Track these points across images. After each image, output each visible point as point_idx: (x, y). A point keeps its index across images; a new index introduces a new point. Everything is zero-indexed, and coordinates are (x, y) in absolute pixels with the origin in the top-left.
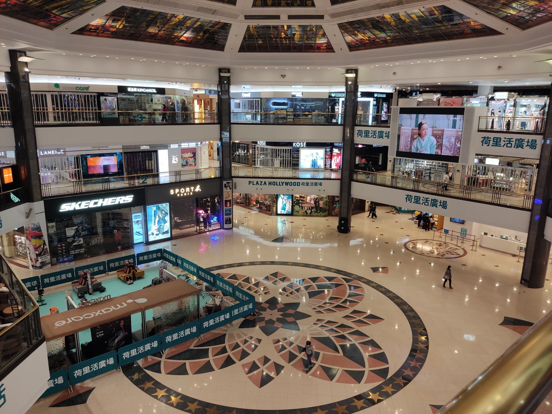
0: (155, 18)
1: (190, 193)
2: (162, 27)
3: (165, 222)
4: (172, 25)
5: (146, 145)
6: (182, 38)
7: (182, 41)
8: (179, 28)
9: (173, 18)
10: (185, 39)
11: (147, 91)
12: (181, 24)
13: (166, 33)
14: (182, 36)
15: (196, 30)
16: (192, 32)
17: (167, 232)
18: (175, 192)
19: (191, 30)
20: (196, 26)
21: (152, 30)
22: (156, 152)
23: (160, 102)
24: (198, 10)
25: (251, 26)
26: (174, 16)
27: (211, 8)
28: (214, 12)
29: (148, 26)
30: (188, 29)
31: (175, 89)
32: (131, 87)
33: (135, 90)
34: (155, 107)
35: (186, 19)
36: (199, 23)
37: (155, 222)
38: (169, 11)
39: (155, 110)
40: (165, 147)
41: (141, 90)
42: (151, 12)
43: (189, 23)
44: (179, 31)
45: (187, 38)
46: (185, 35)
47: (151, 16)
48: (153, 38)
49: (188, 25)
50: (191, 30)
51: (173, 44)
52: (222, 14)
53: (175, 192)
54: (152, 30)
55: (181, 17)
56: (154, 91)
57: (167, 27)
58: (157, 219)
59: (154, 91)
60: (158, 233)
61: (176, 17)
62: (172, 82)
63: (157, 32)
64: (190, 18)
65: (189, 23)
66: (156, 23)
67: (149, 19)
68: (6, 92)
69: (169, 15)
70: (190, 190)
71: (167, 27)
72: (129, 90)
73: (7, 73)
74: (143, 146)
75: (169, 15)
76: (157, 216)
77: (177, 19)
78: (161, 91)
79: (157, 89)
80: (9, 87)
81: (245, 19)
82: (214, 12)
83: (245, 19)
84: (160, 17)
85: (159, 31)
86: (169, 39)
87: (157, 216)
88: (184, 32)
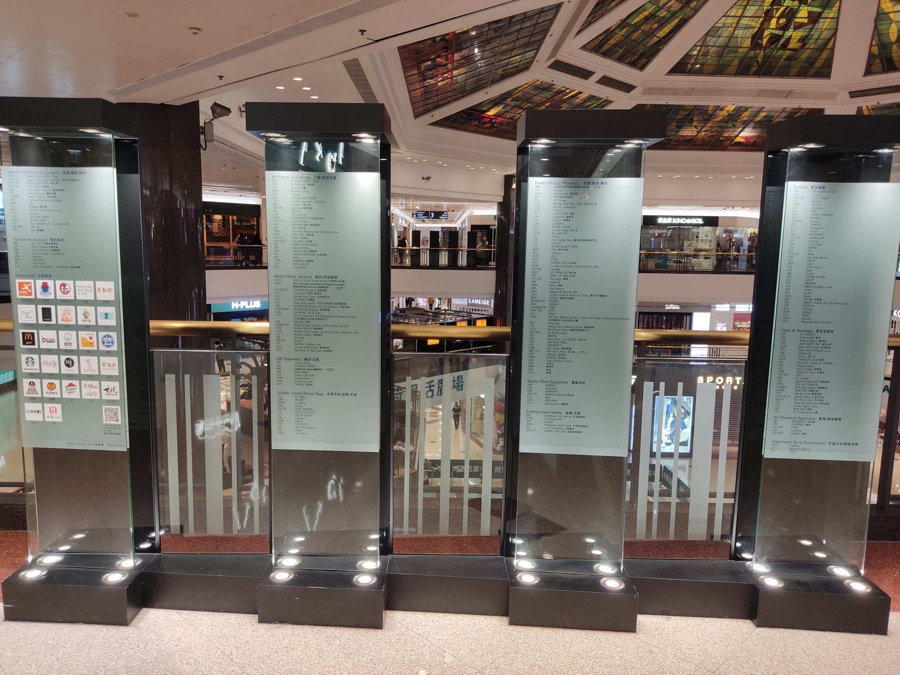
0: (688, 115)
1: (733, 386)
2: (702, 127)
3: (684, 427)
4: (718, 122)
5: (674, 303)
6: (738, 139)
7: (739, 144)
8: (730, 125)
9: (717, 112)
10: (742, 140)
11: (688, 221)
12: (734, 118)
13: (709, 134)
14: (737, 136)
15: (758, 125)
16: (754, 128)
17: (684, 444)
18: (705, 381)
19: (752, 125)
20: (758, 119)
21: (688, 132)
22: (691, 314)
23: (708, 238)
24: (758, 96)
25: (864, 108)
26: (719, 108)
27: (781, 89)
28: (789, 94)
29: (680, 127)
30: (745, 124)
31: (735, 218)
32: (663, 217)
33: (669, 221)
34: (701, 246)
35: (739, 111)
36: (763, 114)
37: (666, 424)
38: (710, 102)
39: (702, 250)
40: (707, 308)
41: (679, 221)
42: (679, 108)
43: (745, 116)
44: (732, 130)
45: (746, 138)
46: (742, 134)
47: (682, 113)
48: (690, 144)
49: (745, 119)
50: (752, 125)
51: (724, 149)
52: (805, 95)
53: (705, 381)
54: (688, 132)
55: (731, 108)
56: (700, 221)
57: (709, 125)
58: (671, 419)
59: (700, 221)
60: (670, 441)
61: (722, 109)
62: (728, 207)
63: (695, 134)
64: (747, 109)
65: (745, 116)
66: (692, 121)
67: (679, 117)
68: (496, 227)
69: (710, 109)
70: (735, 382)
71: (709, 125)
72: (660, 221)
73: (499, 203)
74: (669, 304)
75: (710, 109)
76: (671, 415)
77: (724, 112)
78: (711, 222)
79: (704, 218)
80: (500, 221)
81: (851, 97)
82: (789, 94)
83: (851, 97)
84: (696, 113)
85: (698, 132)
86: (717, 143)
87: (671, 415)
88: (740, 129)
